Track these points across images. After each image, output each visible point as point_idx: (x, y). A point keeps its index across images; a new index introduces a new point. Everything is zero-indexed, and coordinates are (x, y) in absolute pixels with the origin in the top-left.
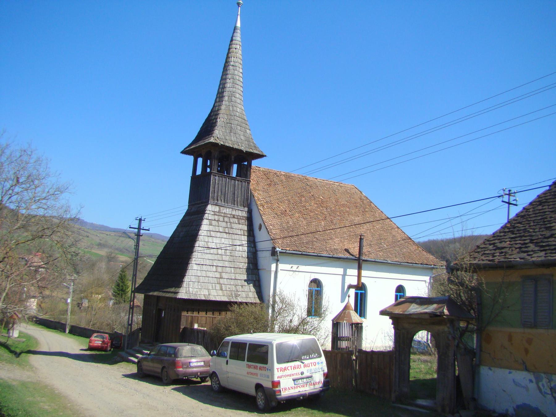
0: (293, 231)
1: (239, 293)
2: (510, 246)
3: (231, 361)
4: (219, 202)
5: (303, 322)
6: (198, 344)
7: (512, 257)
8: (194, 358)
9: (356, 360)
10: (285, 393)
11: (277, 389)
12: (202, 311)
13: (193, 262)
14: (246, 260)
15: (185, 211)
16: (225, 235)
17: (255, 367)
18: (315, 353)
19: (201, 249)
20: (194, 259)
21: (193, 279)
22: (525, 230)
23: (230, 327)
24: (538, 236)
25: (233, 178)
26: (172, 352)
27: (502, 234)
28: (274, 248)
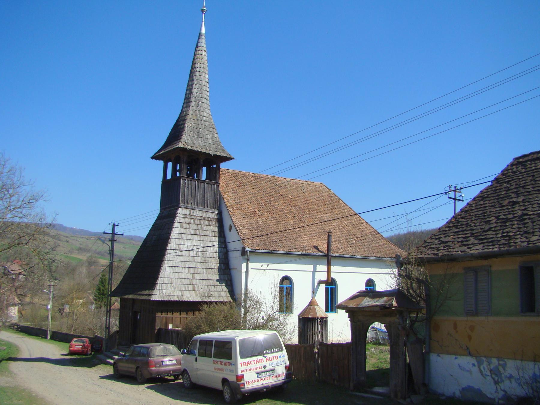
0: (262, 231)
1: (211, 293)
2: (453, 240)
3: (200, 359)
4: (190, 205)
5: (271, 319)
6: (172, 344)
7: (454, 250)
8: (166, 358)
9: (318, 353)
10: (249, 386)
11: (241, 382)
12: (176, 311)
13: (166, 265)
14: (218, 261)
15: (157, 215)
16: (196, 237)
17: (221, 363)
18: (276, 347)
19: (173, 251)
20: (166, 262)
21: (166, 280)
22: (467, 225)
23: (201, 326)
24: (478, 229)
25: (203, 182)
26: (146, 353)
27: (447, 229)
28: (244, 248)
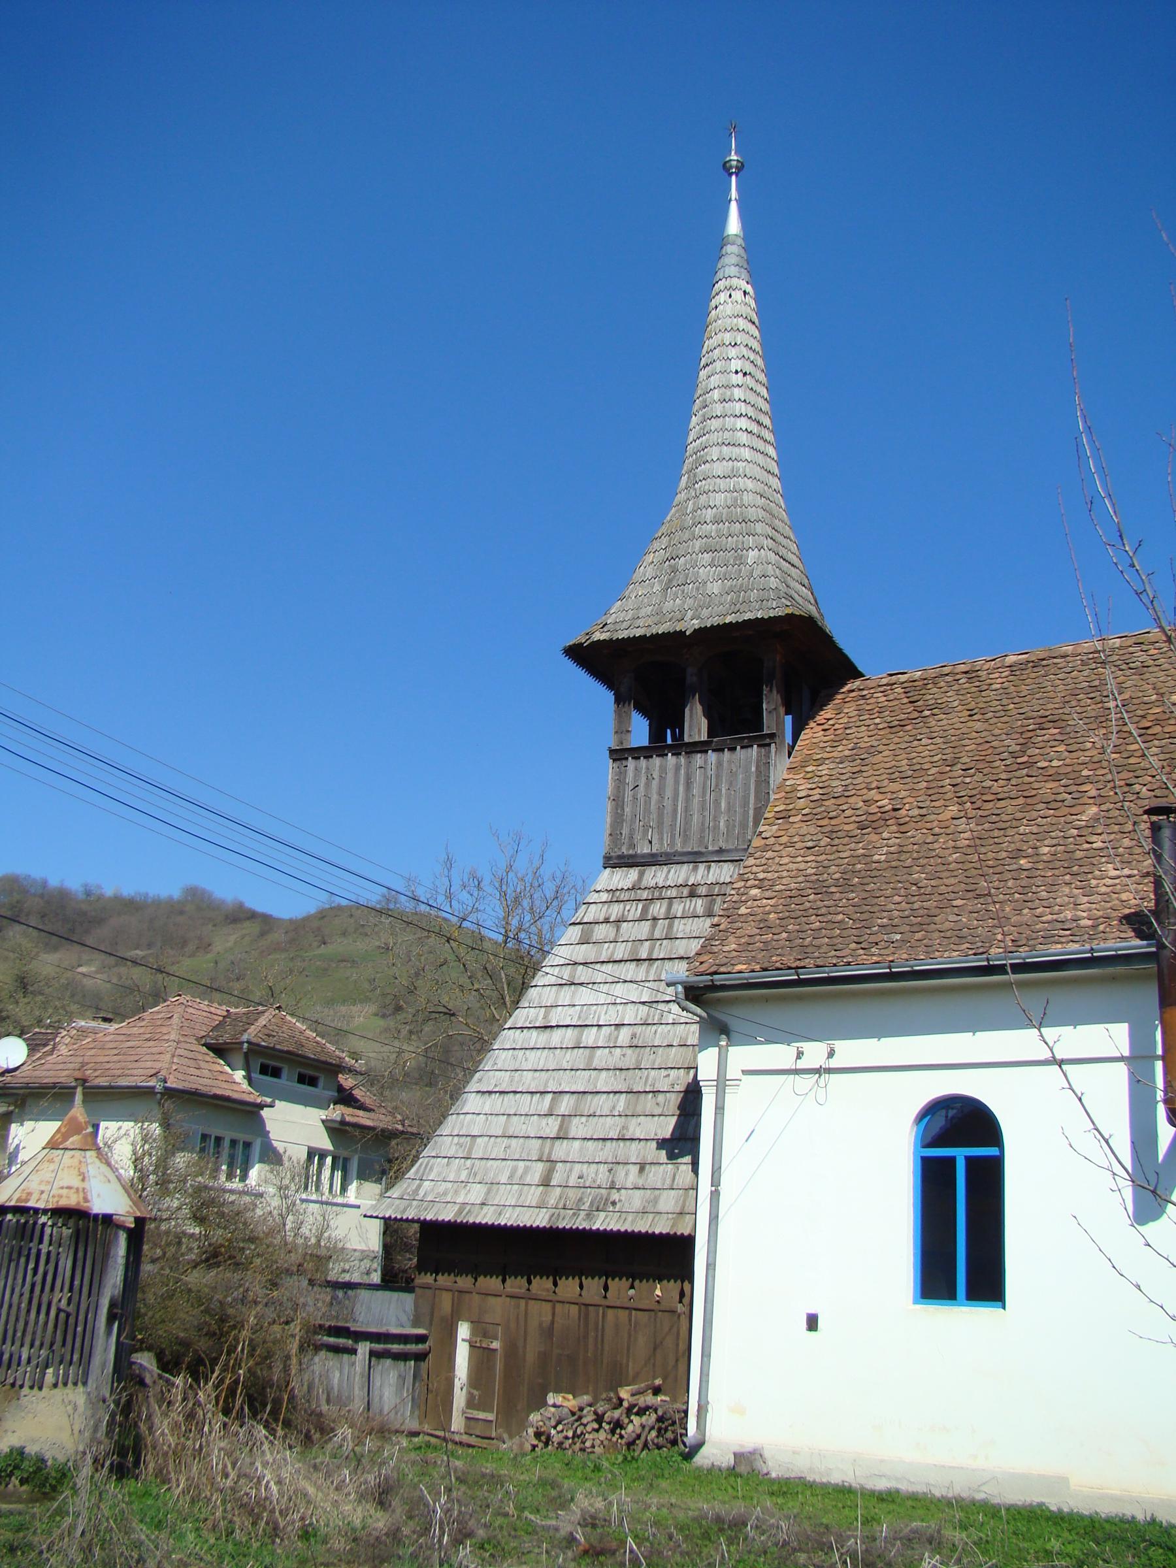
1: (615, 1196)
